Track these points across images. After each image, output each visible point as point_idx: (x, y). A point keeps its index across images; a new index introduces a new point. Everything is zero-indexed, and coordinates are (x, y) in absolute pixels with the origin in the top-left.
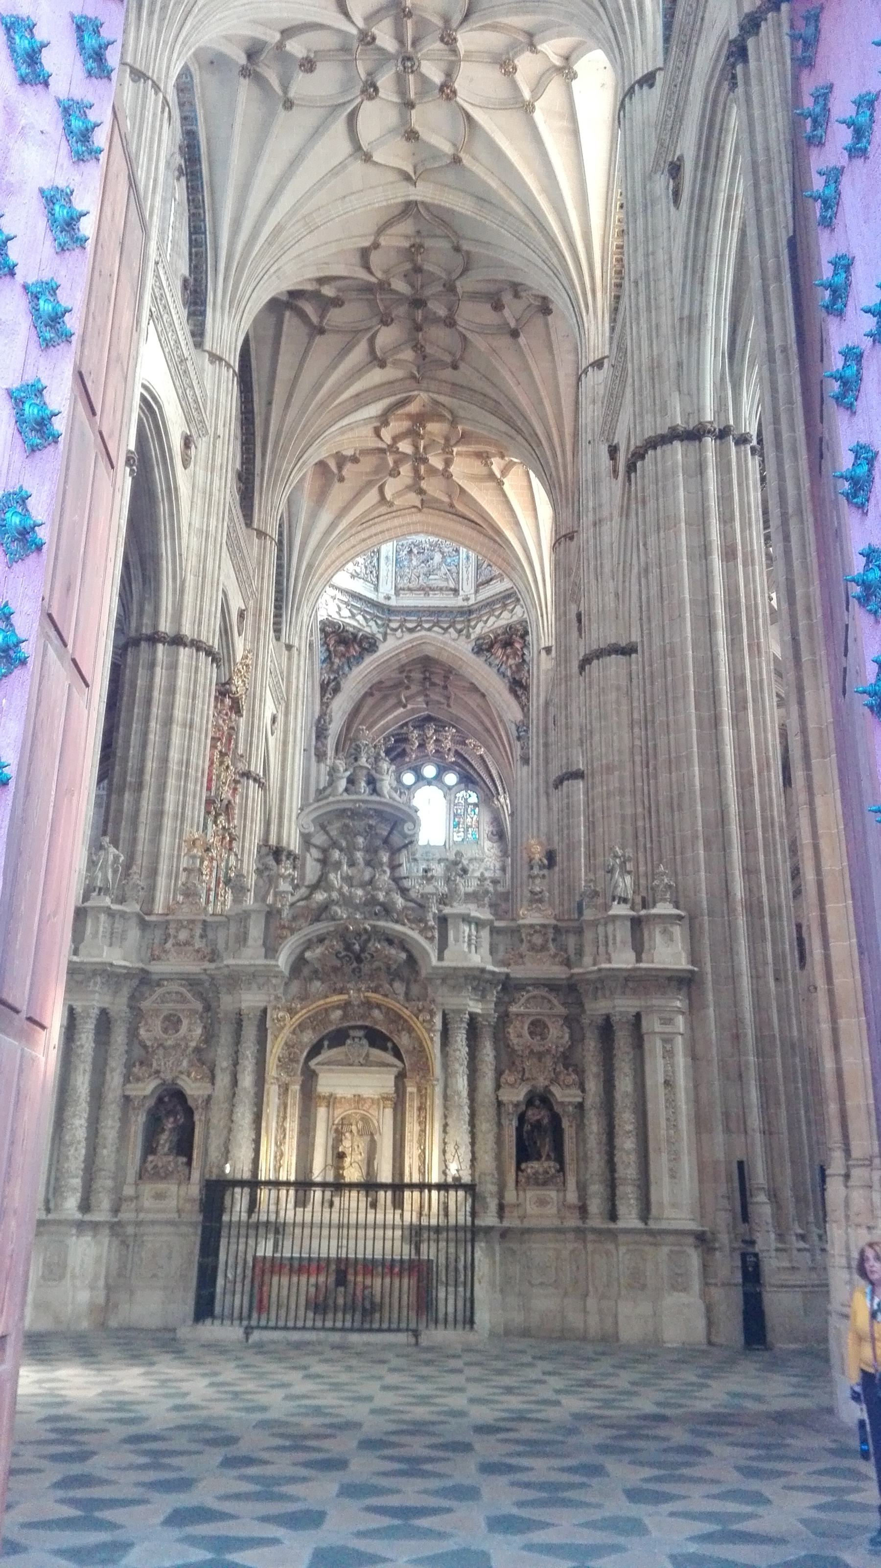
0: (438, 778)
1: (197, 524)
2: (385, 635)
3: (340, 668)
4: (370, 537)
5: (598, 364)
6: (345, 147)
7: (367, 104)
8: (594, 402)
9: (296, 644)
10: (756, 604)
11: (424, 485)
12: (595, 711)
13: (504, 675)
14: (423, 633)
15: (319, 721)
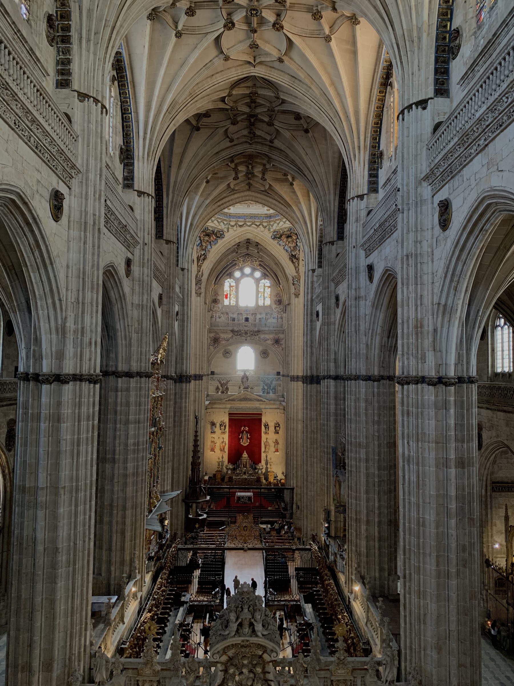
0: (251, 275)
1: (136, 302)
2: (228, 229)
3: (206, 247)
4: (223, 204)
5: (361, 197)
6: (214, 52)
7: (226, 32)
8: (357, 221)
9: (186, 268)
10: (473, 493)
11: (251, 181)
12: (353, 411)
13: (287, 251)
14: (247, 228)
15: (196, 276)
